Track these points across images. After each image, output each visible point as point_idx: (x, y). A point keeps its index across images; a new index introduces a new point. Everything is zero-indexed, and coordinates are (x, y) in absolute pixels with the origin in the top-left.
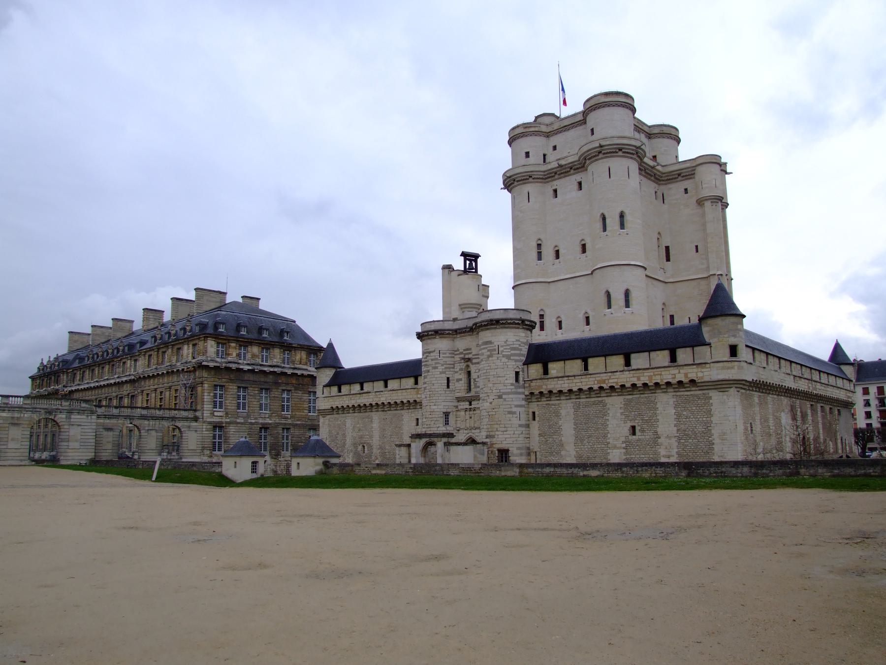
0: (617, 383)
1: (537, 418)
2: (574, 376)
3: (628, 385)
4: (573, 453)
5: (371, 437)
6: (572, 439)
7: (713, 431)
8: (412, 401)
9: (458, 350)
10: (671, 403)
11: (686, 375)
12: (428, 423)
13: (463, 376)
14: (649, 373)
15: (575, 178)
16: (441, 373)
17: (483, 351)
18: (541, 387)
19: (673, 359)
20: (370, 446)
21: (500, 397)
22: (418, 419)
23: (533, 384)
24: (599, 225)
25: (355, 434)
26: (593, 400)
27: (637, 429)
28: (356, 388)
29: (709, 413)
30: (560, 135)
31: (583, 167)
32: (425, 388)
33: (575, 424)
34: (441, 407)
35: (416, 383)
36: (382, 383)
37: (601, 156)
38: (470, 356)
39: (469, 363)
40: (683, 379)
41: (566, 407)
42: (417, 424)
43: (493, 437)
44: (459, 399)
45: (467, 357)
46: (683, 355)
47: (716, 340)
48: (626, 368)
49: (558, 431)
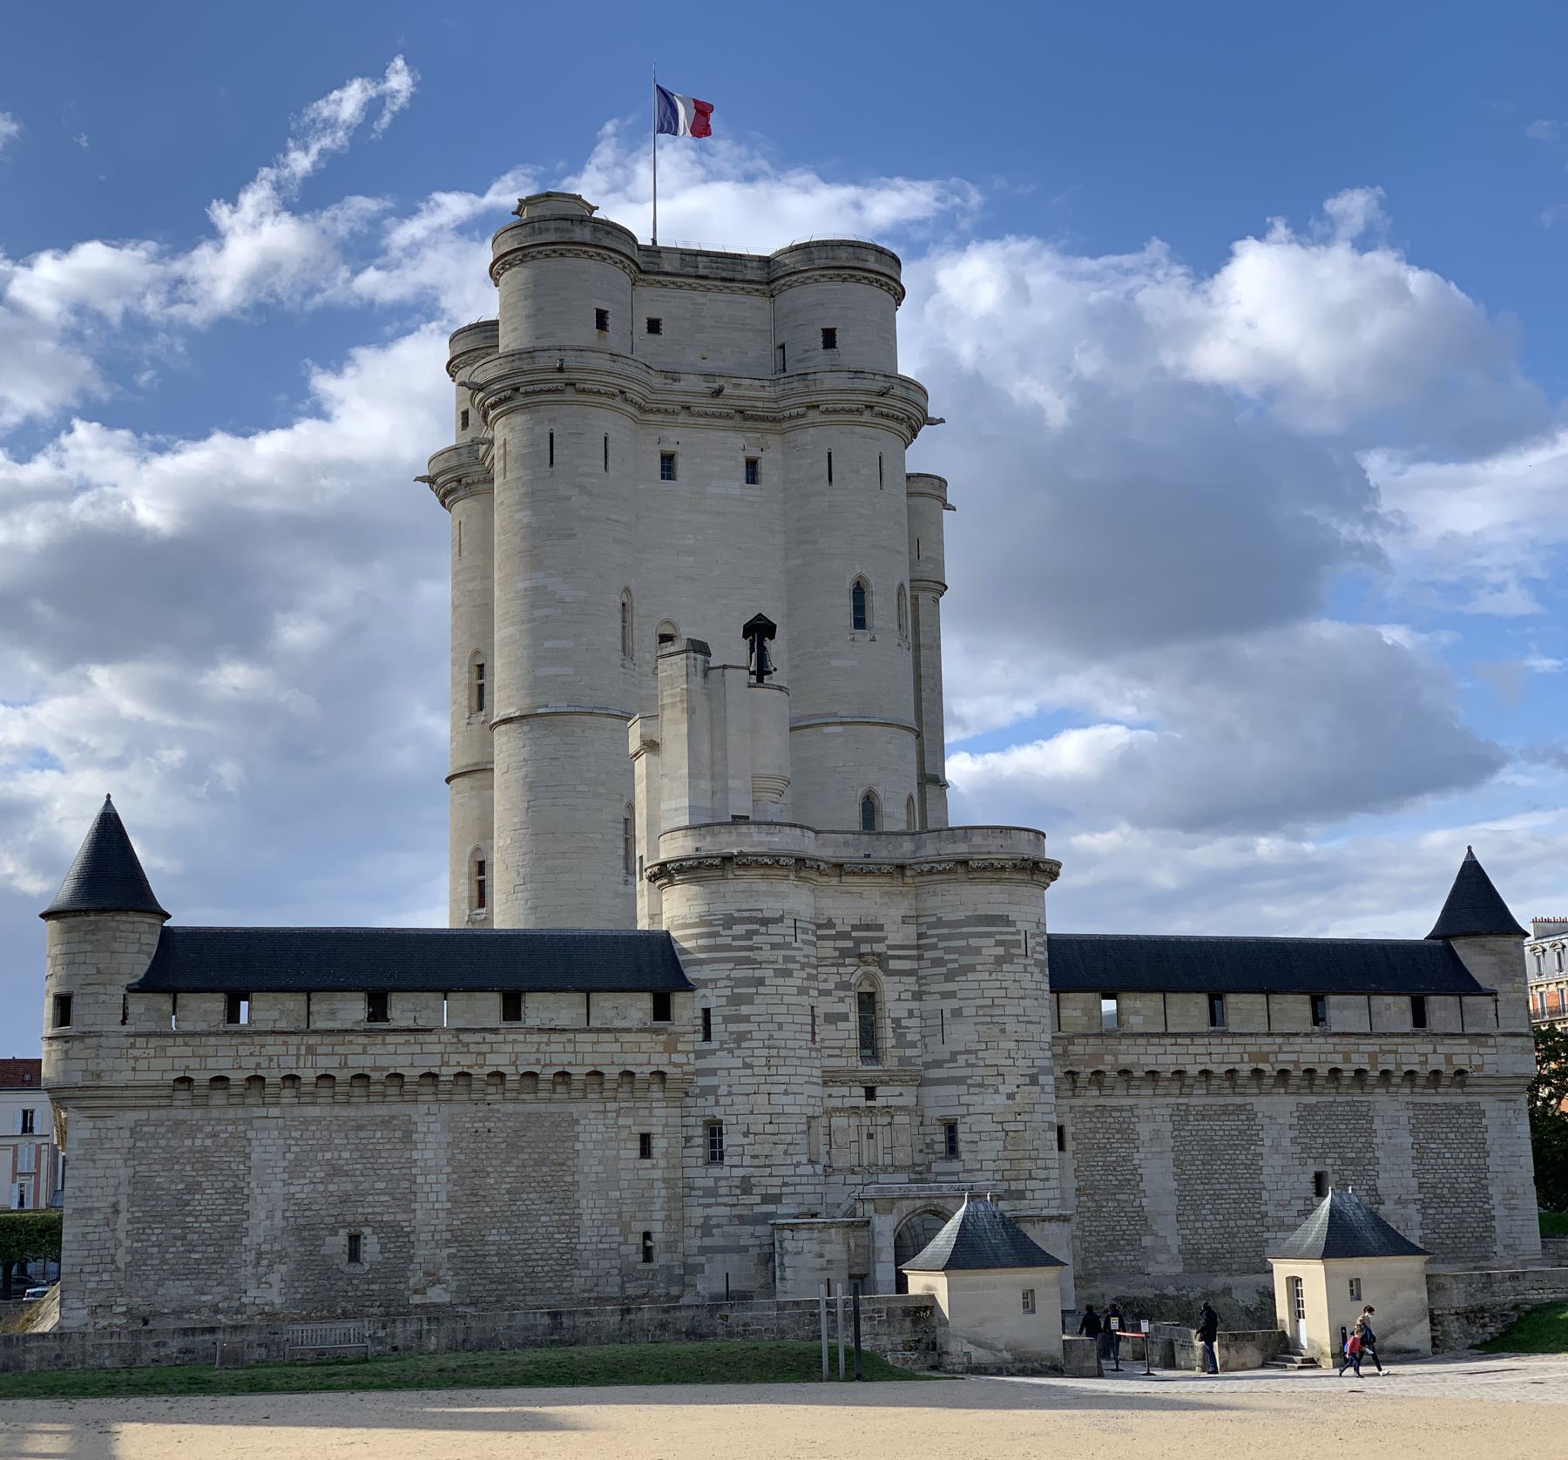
0: (1296, 1063)
1: (1070, 1145)
2: (1192, 1035)
3: (1323, 1071)
4: (1174, 1242)
5: (406, 1201)
6: (1170, 1205)
7: (1491, 1190)
8: (643, 1072)
9: (830, 924)
10: (1404, 1120)
11: (1448, 1058)
12: (757, 1149)
13: (850, 1007)
14: (1369, 1046)
15: (736, 444)
16: (802, 991)
17: (974, 942)
18: (1098, 1057)
19: (1419, 1019)
20: (398, 1237)
21: (1034, 1080)
22: (645, 1139)
23: (1077, 1048)
24: (847, 604)
25: (301, 1190)
26: (1221, 1101)
27: (1332, 1178)
28: (354, 1009)
29: (1482, 1148)
30: (678, 293)
31: (775, 420)
32: (740, 1038)
33: (1177, 1163)
34: (801, 1099)
35: (662, 1011)
36: (489, 1005)
37: (866, 417)
38: (879, 948)
39: (873, 969)
40: (1443, 1068)
41: (1152, 1116)
42: (645, 1152)
43: (1020, 1195)
44: (830, 1079)
45: (865, 948)
46: (1441, 1009)
47: (1508, 986)
48: (1316, 1028)
49: (1131, 1181)
